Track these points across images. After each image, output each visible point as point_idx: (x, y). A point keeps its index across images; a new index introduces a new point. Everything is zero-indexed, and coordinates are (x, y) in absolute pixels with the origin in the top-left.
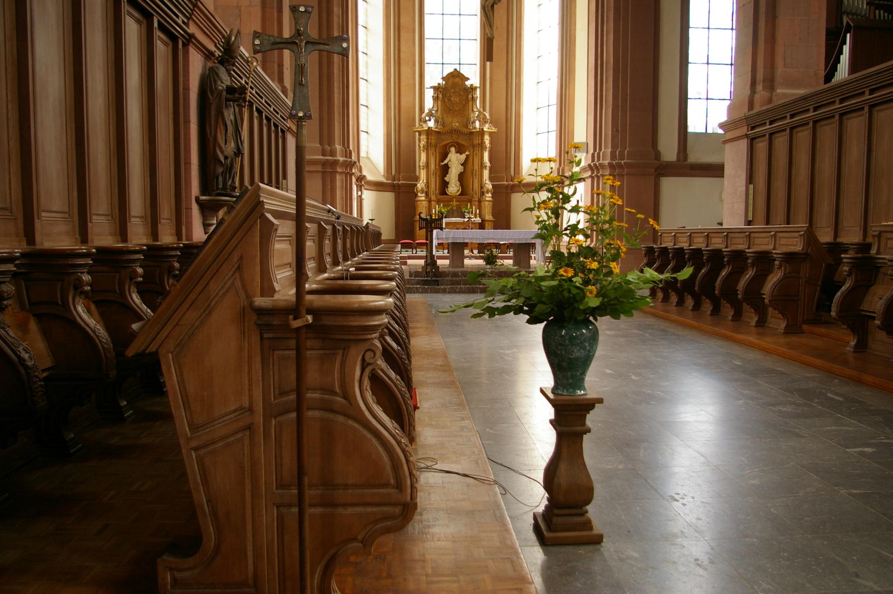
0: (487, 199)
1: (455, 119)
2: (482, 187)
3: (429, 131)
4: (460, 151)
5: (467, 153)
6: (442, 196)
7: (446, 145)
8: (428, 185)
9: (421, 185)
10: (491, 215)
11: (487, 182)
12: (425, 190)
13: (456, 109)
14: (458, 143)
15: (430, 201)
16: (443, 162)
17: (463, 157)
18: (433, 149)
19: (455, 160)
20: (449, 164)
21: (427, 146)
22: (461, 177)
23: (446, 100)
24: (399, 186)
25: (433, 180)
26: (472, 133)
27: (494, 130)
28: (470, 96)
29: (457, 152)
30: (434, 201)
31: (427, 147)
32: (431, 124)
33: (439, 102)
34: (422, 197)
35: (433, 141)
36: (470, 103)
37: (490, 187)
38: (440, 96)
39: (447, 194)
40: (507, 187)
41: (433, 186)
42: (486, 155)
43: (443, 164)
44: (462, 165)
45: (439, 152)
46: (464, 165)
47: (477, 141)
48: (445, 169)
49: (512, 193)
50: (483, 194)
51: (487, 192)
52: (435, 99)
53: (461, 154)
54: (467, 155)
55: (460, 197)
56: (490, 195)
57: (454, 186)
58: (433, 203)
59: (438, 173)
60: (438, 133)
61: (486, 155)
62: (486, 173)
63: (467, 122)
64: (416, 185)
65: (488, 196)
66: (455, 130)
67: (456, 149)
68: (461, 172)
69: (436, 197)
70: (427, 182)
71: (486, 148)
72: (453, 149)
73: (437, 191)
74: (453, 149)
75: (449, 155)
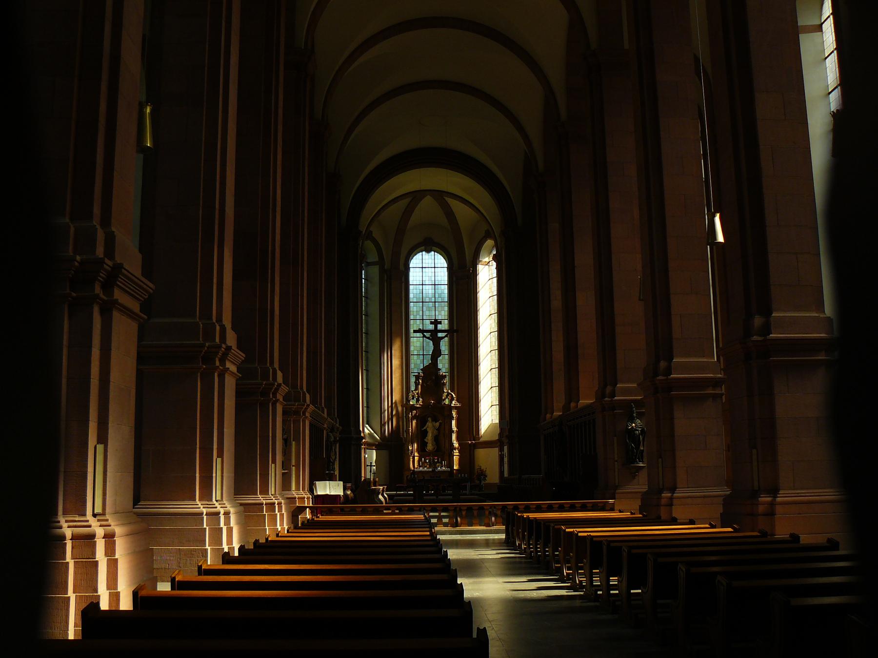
4: (435, 420)
11: (455, 442)
16: (423, 428)
17: (437, 424)
22: (436, 439)
27: (458, 405)
30: (417, 456)
42: (454, 422)
46: (438, 430)
53: (436, 422)
54: (440, 423)
58: (416, 457)
61: (454, 422)
62: (454, 436)
63: (440, 400)
68: (436, 435)
71: (454, 418)
72: (429, 419)
75: (427, 423)
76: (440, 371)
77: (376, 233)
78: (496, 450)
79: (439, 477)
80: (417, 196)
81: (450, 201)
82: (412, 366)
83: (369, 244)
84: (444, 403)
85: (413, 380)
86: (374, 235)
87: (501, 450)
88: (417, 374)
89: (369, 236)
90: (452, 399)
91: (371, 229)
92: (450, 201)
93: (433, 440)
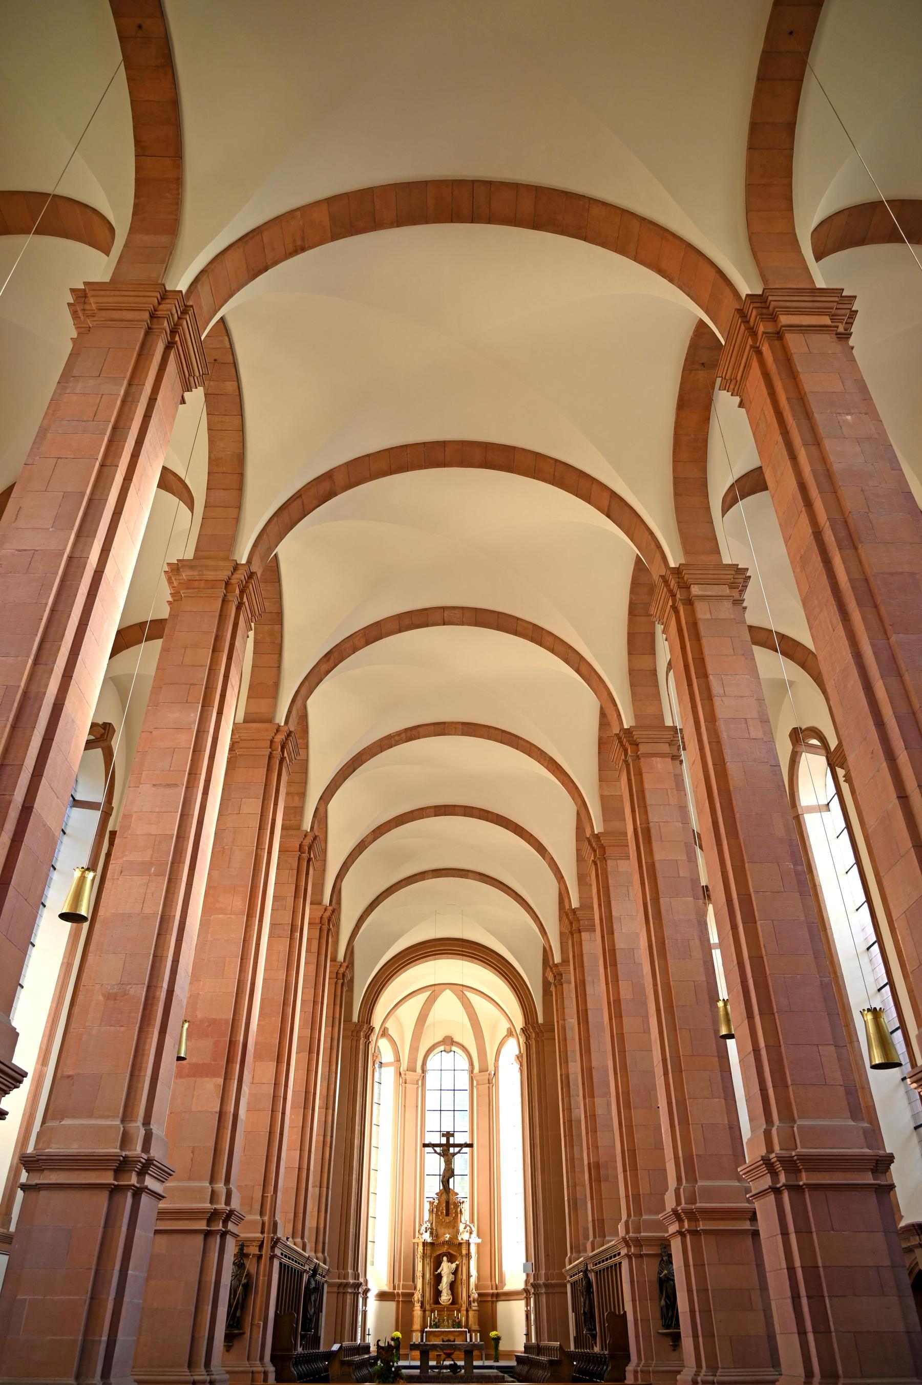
0: (474, 1308)
1: (446, 1231)
2: (469, 1297)
3: (425, 1244)
4: (451, 1260)
5: (457, 1262)
6: (436, 1306)
7: (440, 1255)
8: (423, 1296)
9: (417, 1296)
10: (477, 1324)
11: (474, 1291)
12: (420, 1299)
13: (448, 1221)
14: (449, 1253)
15: (424, 1311)
17: (454, 1266)
18: (428, 1260)
19: (446, 1268)
20: (442, 1273)
21: (423, 1257)
22: (453, 1286)
23: (439, 1213)
24: (398, 1293)
25: (427, 1290)
26: (460, 1244)
28: (459, 1210)
29: (448, 1261)
30: (428, 1311)
31: (424, 1256)
32: (427, 1237)
33: (434, 1215)
34: (417, 1307)
35: (428, 1252)
36: (459, 1215)
37: (476, 1296)
38: (435, 1210)
39: (440, 1304)
40: (492, 1295)
41: (427, 1295)
43: (437, 1273)
44: (453, 1274)
45: (434, 1262)
46: (455, 1273)
47: (464, 1252)
48: (438, 1278)
49: (497, 1301)
50: (470, 1303)
51: (474, 1301)
52: (431, 1211)
53: (452, 1263)
55: (453, 1306)
56: (476, 1304)
57: (446, 1295)
59: (432, 1283)
60: (432, 1244)
64: (412, 1294)
65: (475, 1305)
66: (447, 1241)
67: (448, 1259)
69: (430, 1306)
70: (423, 1292)
72: (445, 1258)
73: (432, 1301)
74: (445, 1258)
76: (458, 1196)
77: (392, 1032)
78: (523, 1302)
79: (454, 1341)
80: (435, 990)
81: (469, 995)
82: (426, 1189)
83: (384, 1045)
84: (462, 1239)
85: (427, 1207)
86: (389, 1033)
87: (528, 1304)
88: (431, 1200)
89: (384, 1033)
90: (471, 1233)
91: (387, 1025)
92: (469, 995)
93: (449, 1288)
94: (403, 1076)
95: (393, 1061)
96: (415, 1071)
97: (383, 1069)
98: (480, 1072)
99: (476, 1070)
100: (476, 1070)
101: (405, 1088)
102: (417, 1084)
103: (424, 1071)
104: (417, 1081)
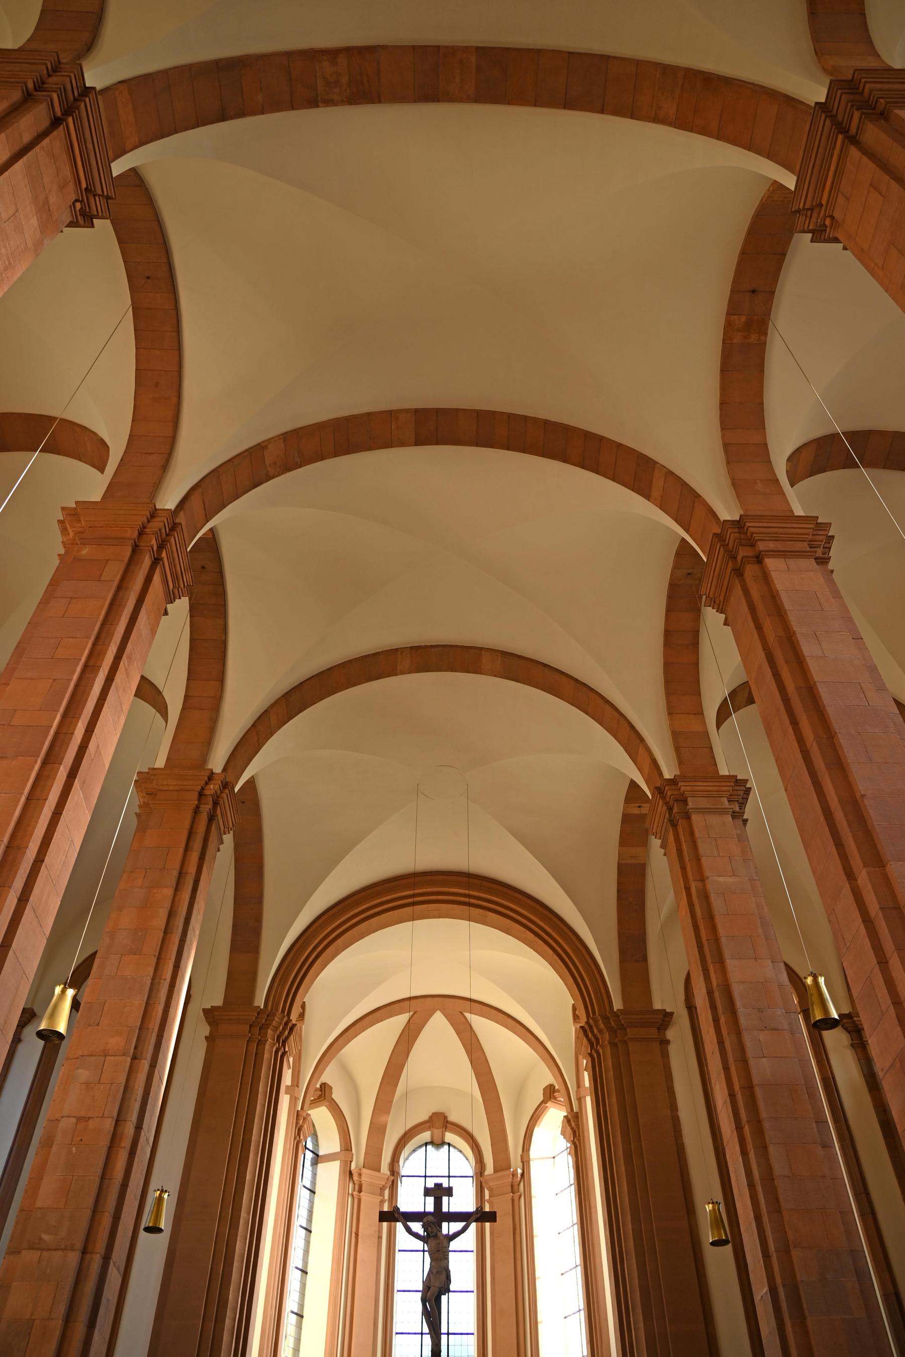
92: (479, 1023)
94: (355, 1178)
95: (338, 1150)
96: (379, 1170)
97: (320, 1166)
98: (496, 1170)
99: (489, 1169)
100: (489, 1169)
101: (359, 1200)
102: (382, 1194)
103: (394, 1171)
104: (382, 1189)
